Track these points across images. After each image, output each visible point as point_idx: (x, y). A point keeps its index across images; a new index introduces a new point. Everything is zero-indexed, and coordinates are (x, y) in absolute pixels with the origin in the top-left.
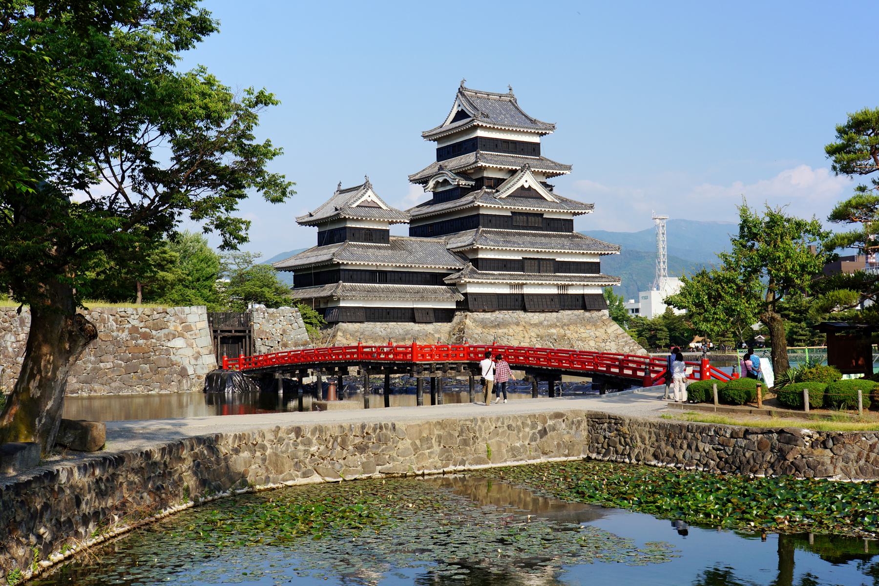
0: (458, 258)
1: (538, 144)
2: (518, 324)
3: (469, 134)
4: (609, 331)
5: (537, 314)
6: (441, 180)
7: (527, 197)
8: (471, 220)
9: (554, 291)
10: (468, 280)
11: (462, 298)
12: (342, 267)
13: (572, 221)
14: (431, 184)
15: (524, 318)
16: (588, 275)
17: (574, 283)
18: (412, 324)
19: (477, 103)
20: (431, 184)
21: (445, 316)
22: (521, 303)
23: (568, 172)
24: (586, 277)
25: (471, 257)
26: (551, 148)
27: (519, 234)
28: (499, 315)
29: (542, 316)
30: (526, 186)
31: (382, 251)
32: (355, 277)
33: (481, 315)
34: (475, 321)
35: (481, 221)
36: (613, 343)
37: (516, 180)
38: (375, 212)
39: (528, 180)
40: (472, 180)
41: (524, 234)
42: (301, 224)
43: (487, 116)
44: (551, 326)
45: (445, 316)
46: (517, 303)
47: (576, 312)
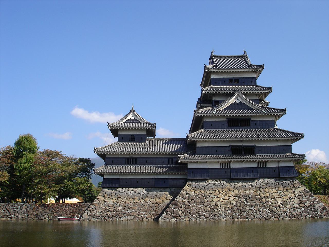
4: (297, 191)
9: (255, 165)
10: (183, 160)
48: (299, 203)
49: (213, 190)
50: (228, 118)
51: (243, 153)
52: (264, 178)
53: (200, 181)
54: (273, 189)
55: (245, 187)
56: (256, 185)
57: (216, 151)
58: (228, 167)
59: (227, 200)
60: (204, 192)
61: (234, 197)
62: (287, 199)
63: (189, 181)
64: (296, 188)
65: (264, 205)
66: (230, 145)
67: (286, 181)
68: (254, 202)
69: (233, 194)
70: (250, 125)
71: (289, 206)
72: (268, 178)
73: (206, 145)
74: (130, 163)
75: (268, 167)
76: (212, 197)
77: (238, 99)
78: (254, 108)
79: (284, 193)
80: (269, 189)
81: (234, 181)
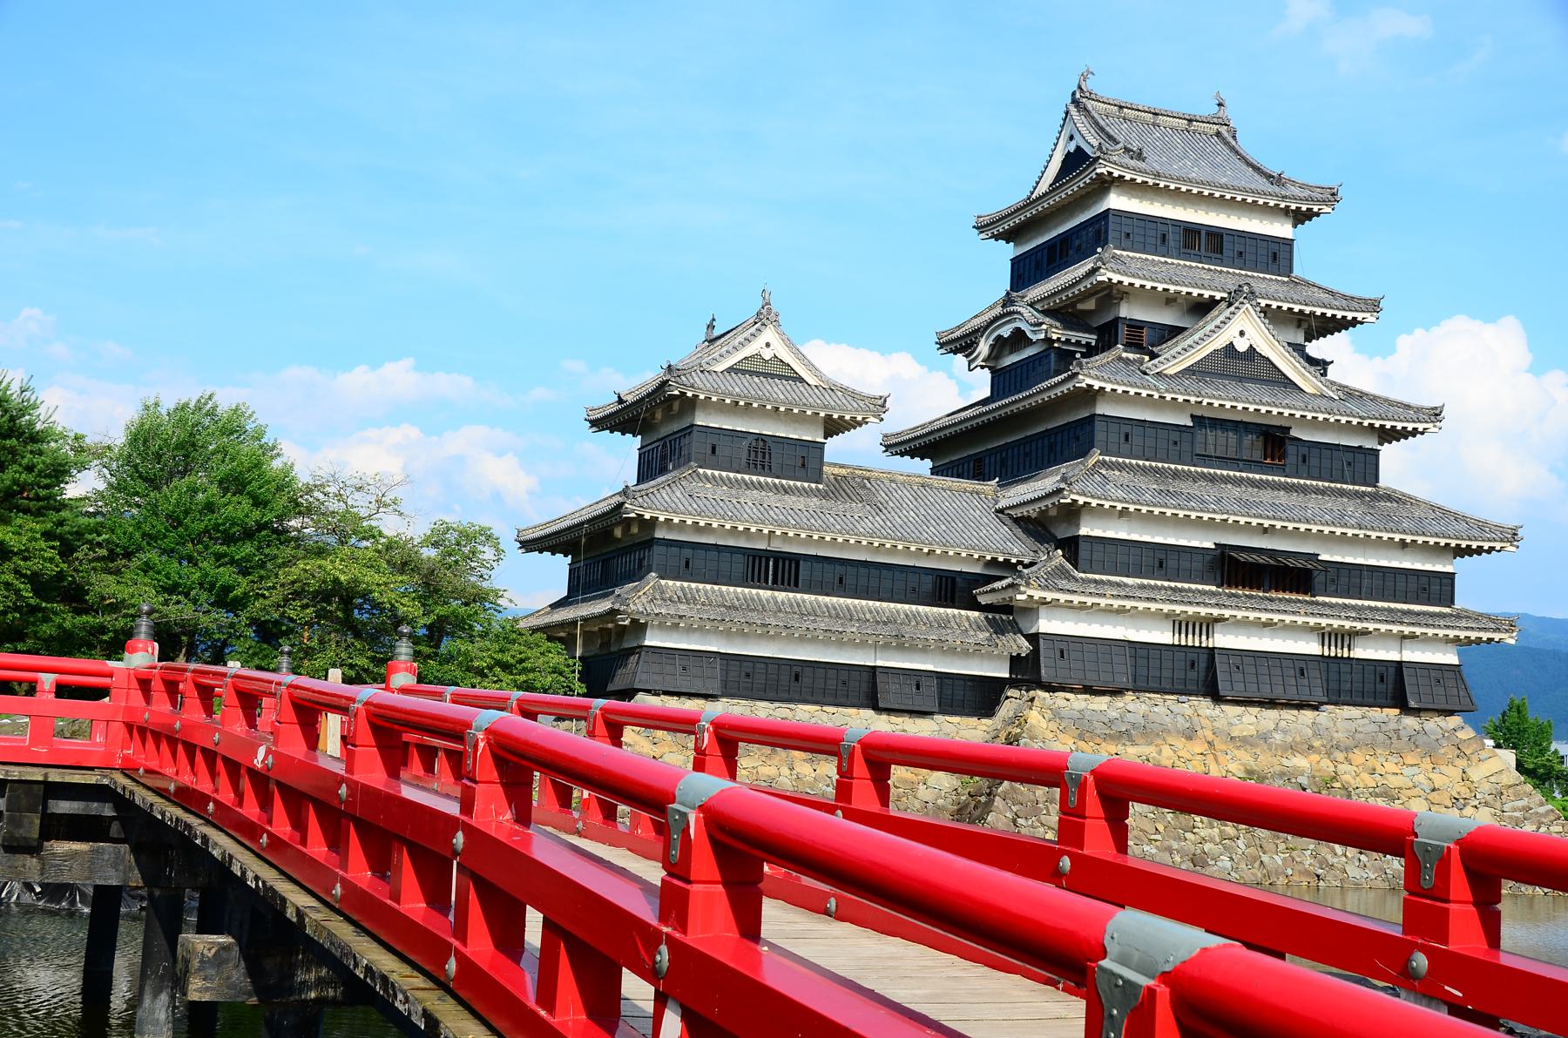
0: (1019, 531)
1: (1289, 243)
2: (1190, 734)
4: (1476, 774)
5: (1254, 710)
6: (1006, 332)
7: (1241, 379)
8: (1066, 433)
9: (1312, 647)
10: (1037, 594)
11: (1025, 647)
12: (659, 534)
13: (1375, 453)
14: (983, 348)
15: (1212, 719)
17: (1371, 626)
18: (870, 713)
19: (1119, 131)
20: (983, 348)
21: (981, 697)
22: (1204, 675)
23: (1369, 317)
24: (1409, 612)
25: (1062, 532)
26: (1324, 259)
27: (1212, 479)
28: (1134, 706)
29: (1269, 718)
30: (1242, 346)
31: (790, 500)
32: (697, 563)
33: (1079, 702)
34: (1057, 715)
35: (1099, 435)
37: (1211, 326)
38: (778, 391)
39: (1244, 329)
40: (1089, 330)
41: (1226, 480)
43: (1139, 156)
44: (1293, 748)
45: (981, 697)
46: (1192, 675)
47: (1376, 713)
77: (1242, 333)
81: (1225, 707)
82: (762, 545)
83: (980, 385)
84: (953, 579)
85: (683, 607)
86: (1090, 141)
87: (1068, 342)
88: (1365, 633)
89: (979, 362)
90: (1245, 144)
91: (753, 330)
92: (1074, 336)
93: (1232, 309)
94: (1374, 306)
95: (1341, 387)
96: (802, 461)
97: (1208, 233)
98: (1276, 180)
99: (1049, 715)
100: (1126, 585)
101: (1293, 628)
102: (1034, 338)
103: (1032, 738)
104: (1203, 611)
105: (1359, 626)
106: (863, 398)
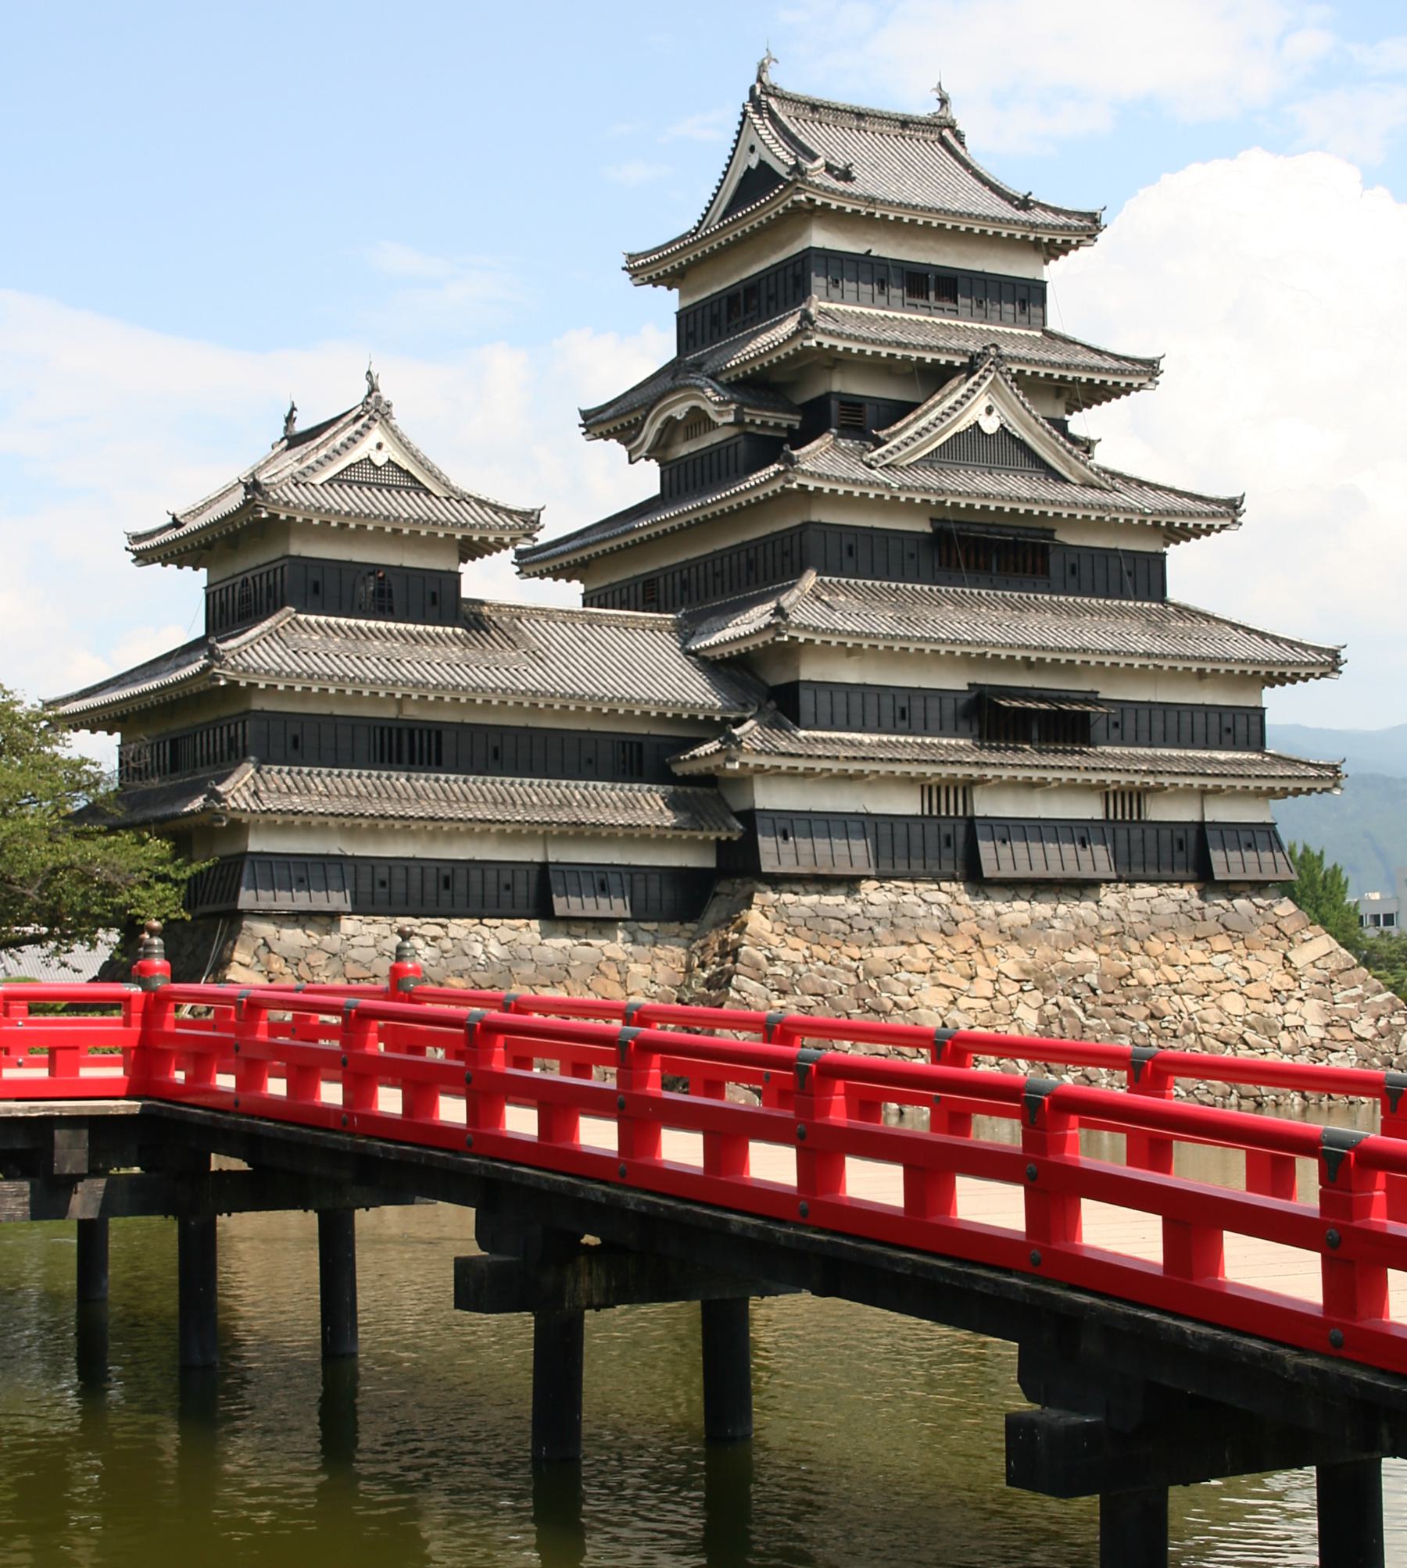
3: (782, 246)
6: (679, 412)
9: (1091, 809)
10: (753, 761)
12: (257, 704)
14: (650, 433)
16: (1222, 756)
17: (1166, 780)
20: (650, 433)
25: (777, 677)
29: (1042, 909)
30: (990, 426)
36: (1312, 1004)
40: (791, 409)
42: (143, 558)
43: (846, 175)
44: (1079, 942)
48: (1328, 1025)
49: (903, 943)
50: (939, 516)
51: (1035, 734)
52: (1131, 882)
53: (820, 888)
54: (1187, 947)
55: (1052, 927)
56: (1102, 918)
57: (901, 711)
58: (960, 813)
59: (988, 999)
60: (856, 953)
61: (1017, 986)
62: (1267, 1002)
63: (761, 887)
64: (1290, 940)
65: (1175, 1031)
66: (969, 685)
67: (1236, 902)
68: (1123, 1015)
69: (1010, 968)
70: (1046, 571)
71: (1285, 1039)
72: (1151, 882)
73: (849, 673)
74: (400, 761)
75: (1151, 822)
76: (908, 983)
78: (1071, 470)
79: (1245, 968)
80: (1168, 945)
81: (989, 892)
82: (391, 713)
83: (644, 480)
84: (640, 745)
85: (296, 799)
86: (781, 157)
87: (764, 424)
88: (1160, 789)
89: (643, 452)
90: (975, 149)
91: (358, 426)
92: (772, 418)
93: (975, 378)
94: (1150, 368)
95: (1114, 475)
96: (435, 600)
97: (938, 278)
98: (1025, 204)
99: (771, 912)
100: (861, 743)
101: (1072, 787)
102: (720, 421)
103: (755, 945)
104: (960, 772)
105: (1151, 781)
106: (510, 513)
